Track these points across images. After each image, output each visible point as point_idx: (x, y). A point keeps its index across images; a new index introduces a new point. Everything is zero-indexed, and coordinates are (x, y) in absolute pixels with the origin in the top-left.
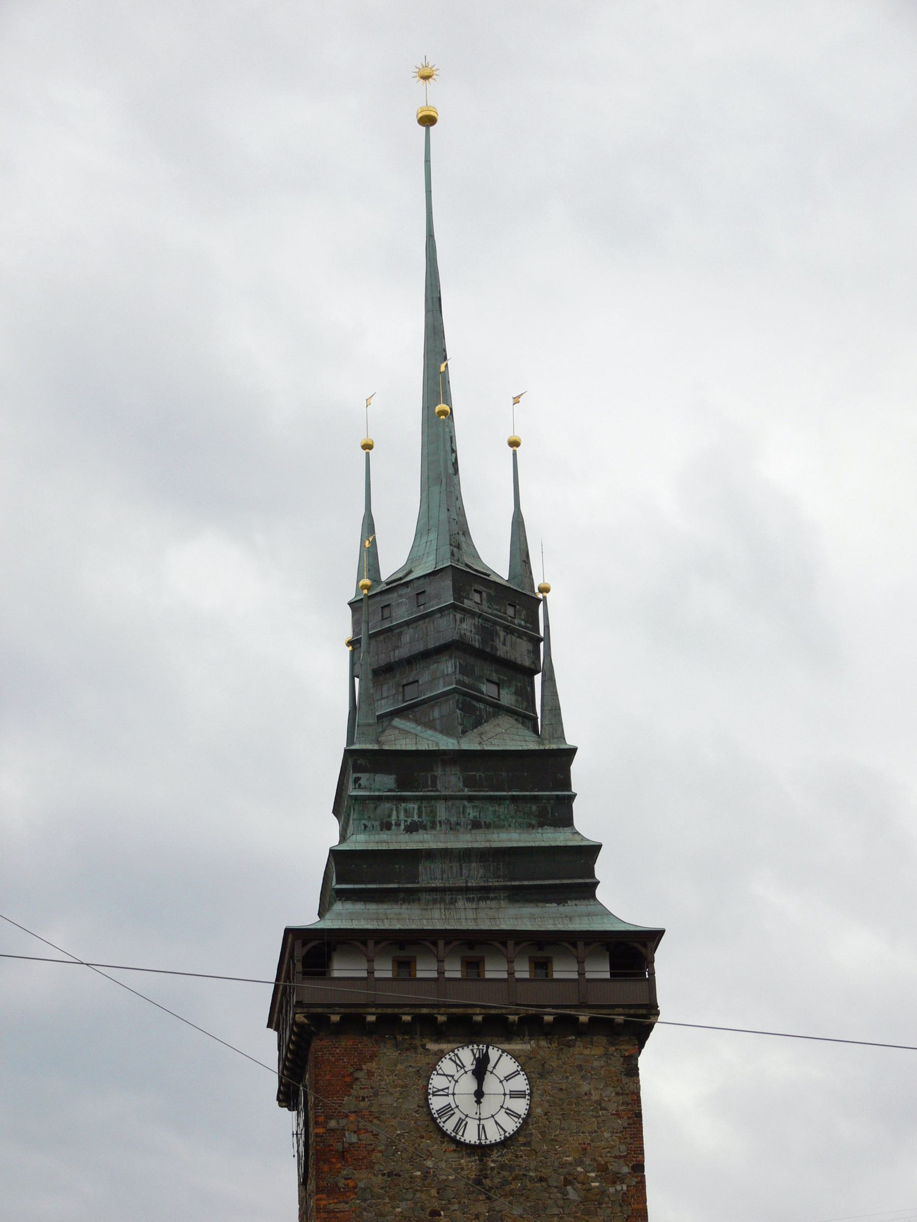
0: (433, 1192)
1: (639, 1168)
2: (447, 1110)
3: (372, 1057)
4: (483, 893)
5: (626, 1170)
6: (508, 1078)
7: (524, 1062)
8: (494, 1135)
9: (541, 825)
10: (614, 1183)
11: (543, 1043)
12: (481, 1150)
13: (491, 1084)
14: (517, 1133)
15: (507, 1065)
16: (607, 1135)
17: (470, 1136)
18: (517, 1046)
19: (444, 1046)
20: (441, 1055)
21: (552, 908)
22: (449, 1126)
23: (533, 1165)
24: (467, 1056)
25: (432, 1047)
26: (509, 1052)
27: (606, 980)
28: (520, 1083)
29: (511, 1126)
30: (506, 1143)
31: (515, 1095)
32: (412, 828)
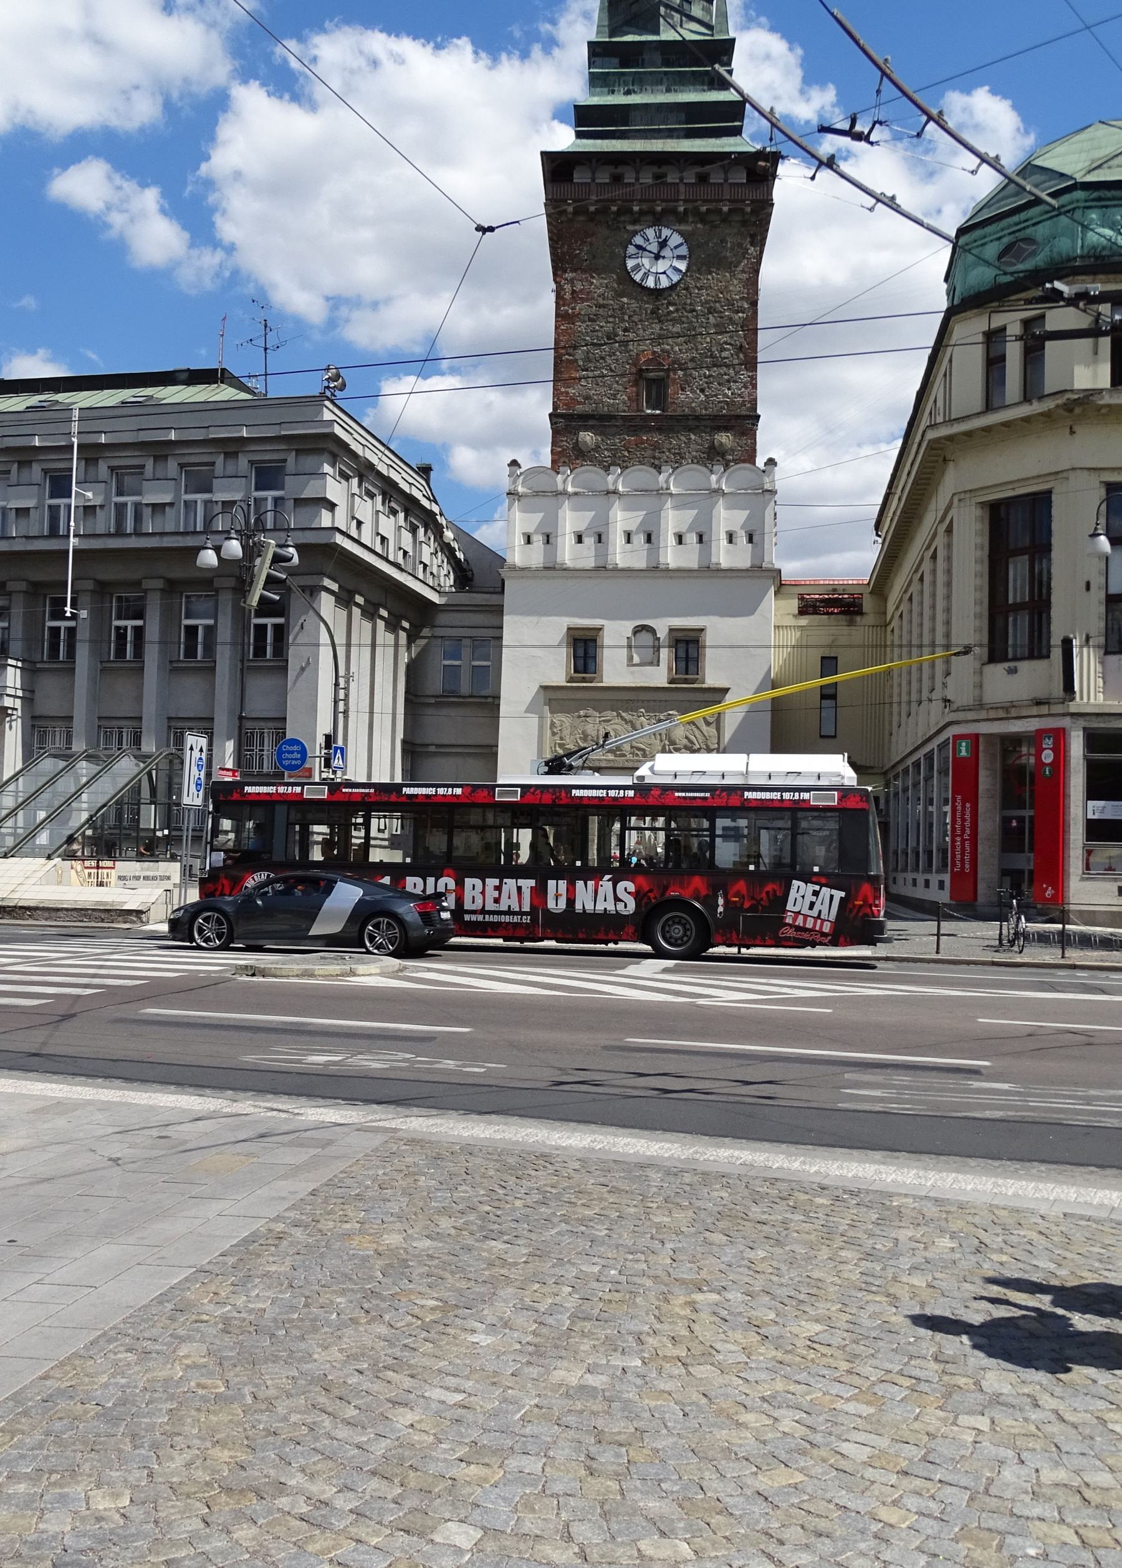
0: (626, 318)
1: (754, 304)
2: (637, 267)
3: (593, 235)
4: (670, 134)
5: (746, 306)
6: (676, 247)
7: (687, 237)
8: (665, 283)
9: (710, 90)
10: (738, 312)
11: (699, 226)
12: (657, 293)
13: (666, 252)
14: (679, 282)
15: (676, 239)
16: (735, 282)
17: (650, 283)
18: (683, 227)
19: (638, 227)
20: (635, 233)
21: (712, 141)
22: (637, 277)
23: (689, 301)
24: (650, 233)
25: (630, 228)
26: (677, 231)
27: (742, 184)
28: (684, 250)
29: (676, 278)
30: (673, 287)
31: (680, 257)
32: (628, 93)
